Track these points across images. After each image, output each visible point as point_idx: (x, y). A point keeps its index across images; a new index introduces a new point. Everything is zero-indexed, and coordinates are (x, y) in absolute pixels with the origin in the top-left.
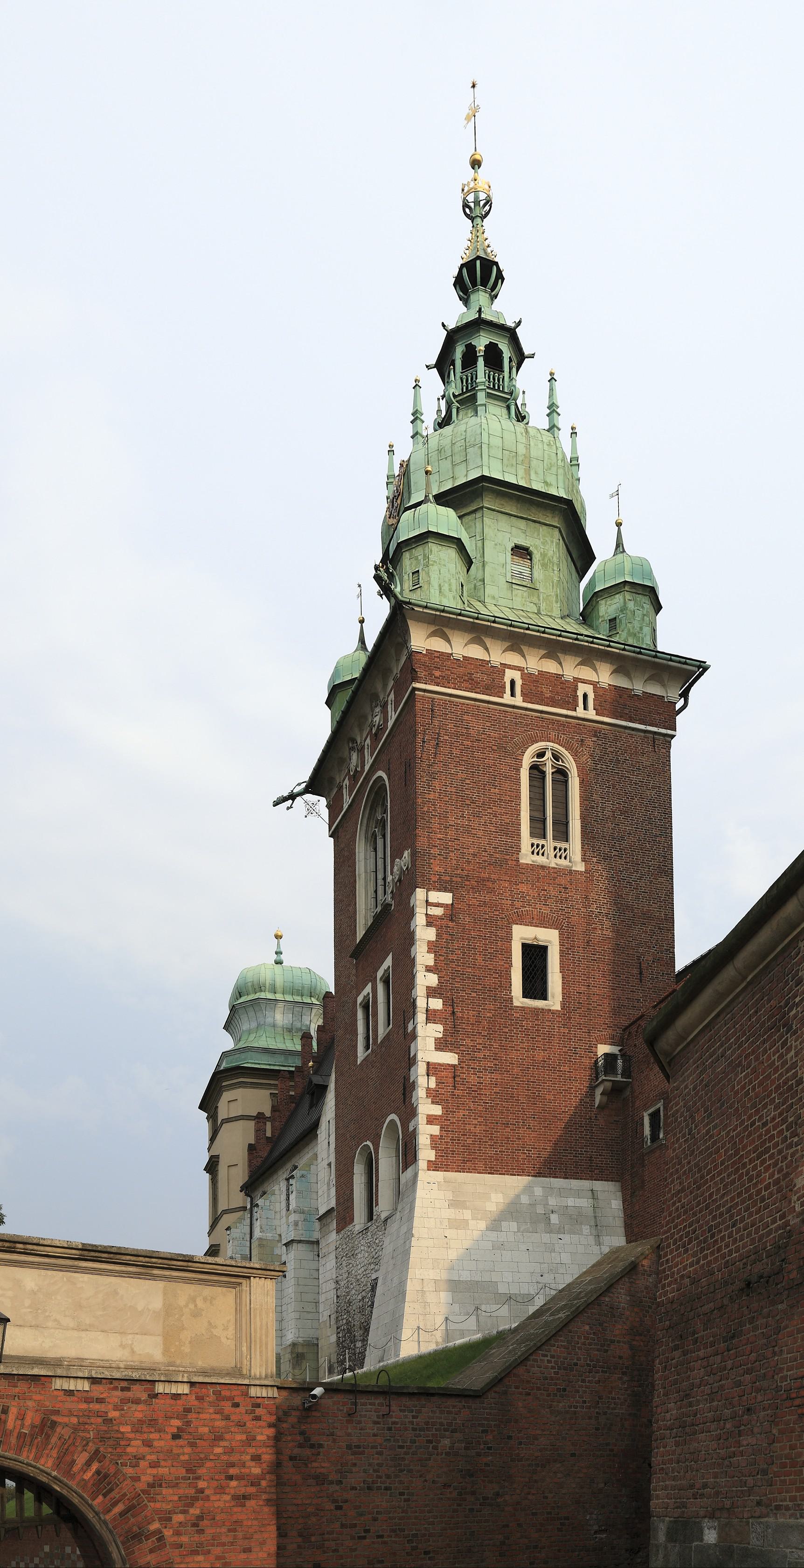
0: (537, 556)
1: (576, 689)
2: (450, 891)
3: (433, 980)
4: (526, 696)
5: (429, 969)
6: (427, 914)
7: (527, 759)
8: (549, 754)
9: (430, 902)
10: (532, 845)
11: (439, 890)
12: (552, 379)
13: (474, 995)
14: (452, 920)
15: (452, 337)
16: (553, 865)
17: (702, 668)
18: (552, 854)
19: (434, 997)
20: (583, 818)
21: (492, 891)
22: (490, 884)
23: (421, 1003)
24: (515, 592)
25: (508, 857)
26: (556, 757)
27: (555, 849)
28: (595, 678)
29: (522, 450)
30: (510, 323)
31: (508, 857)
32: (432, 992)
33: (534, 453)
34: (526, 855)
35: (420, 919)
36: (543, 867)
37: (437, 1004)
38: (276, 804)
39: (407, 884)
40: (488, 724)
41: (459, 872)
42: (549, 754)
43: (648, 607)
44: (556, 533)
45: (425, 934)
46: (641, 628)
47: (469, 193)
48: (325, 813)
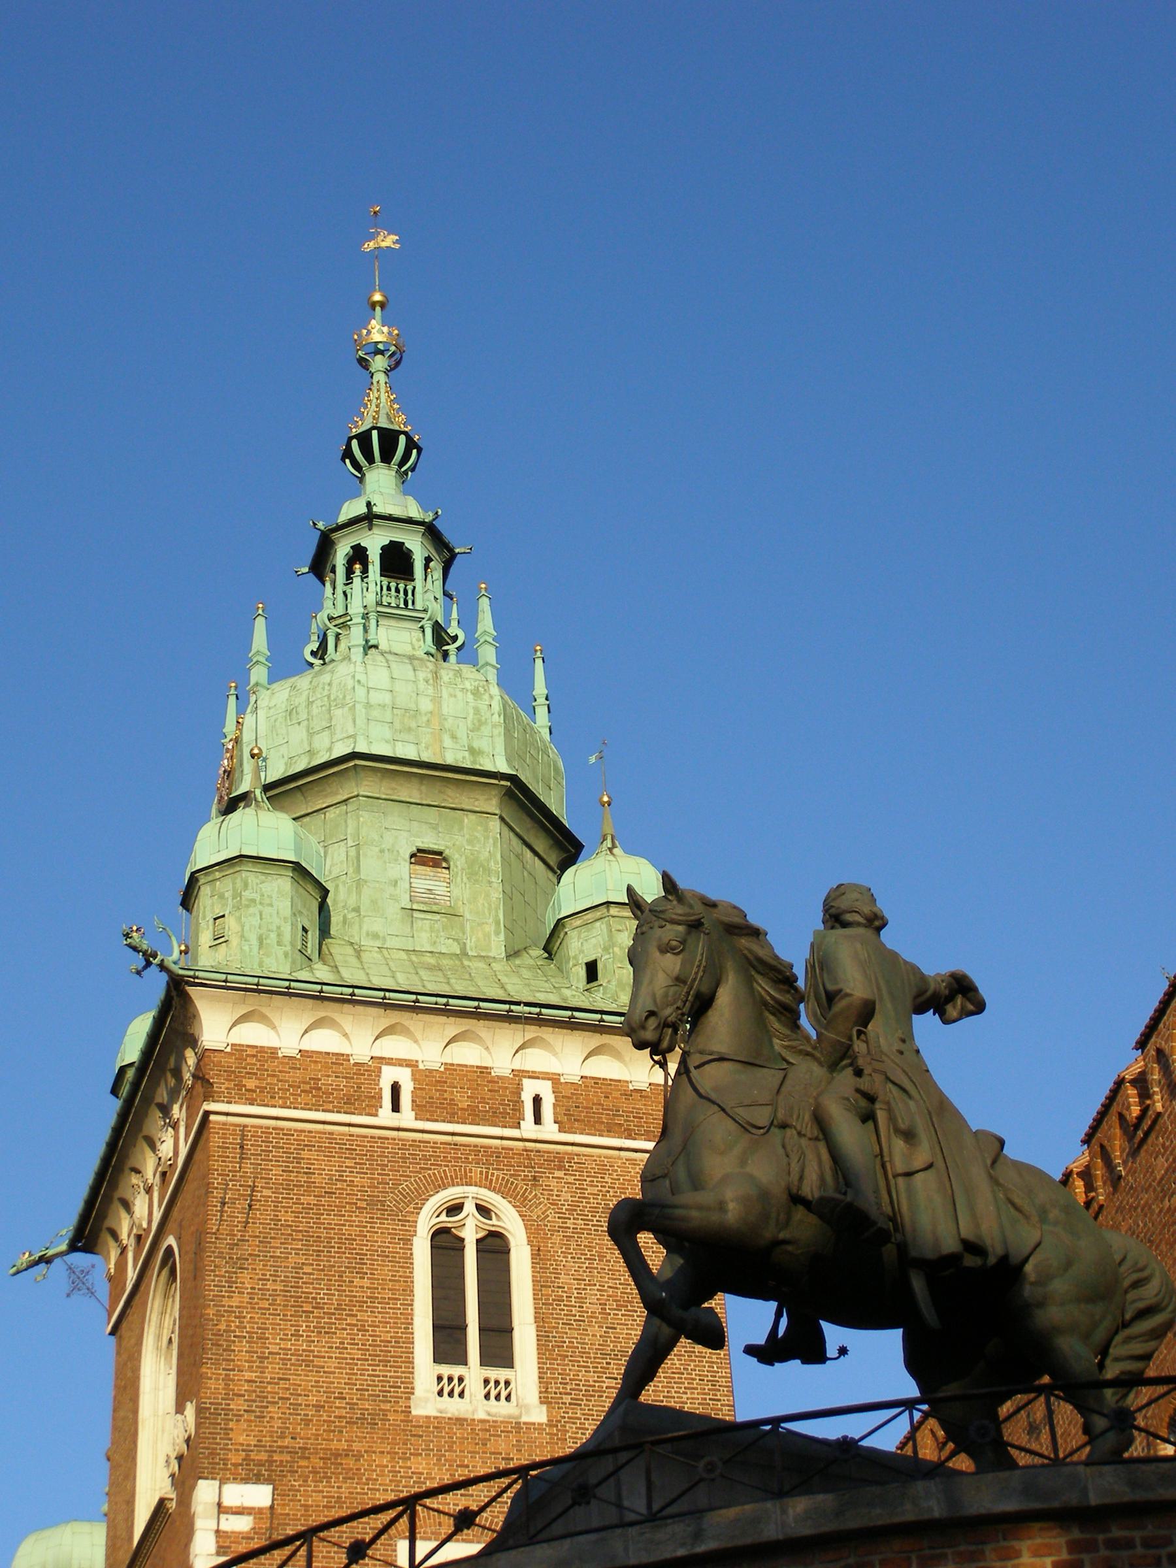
1: (519, 1089)
2: (268, 1481)
4: (421, 1110)
7: (426, 1221)
11: (246, 1480)
21: (352, 1475)
22: (350, 1462)
26: (484, 1210)
34: (427, 1400)
36: (460, 1421)
40: (349, 1163)
41: (287, 1441)
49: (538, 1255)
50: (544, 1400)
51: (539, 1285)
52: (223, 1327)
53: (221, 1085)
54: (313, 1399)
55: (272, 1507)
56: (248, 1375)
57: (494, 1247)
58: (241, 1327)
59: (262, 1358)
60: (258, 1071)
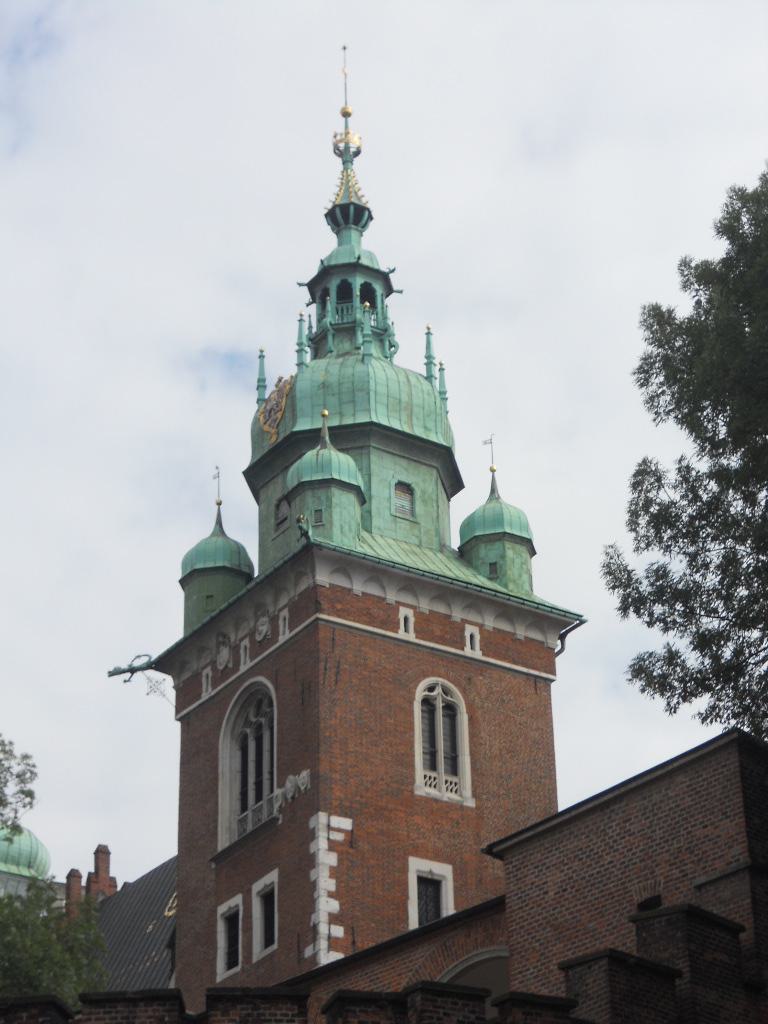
0: (418, 493)
2: (350, 817)
3: (334, 906)
5: (331, 895)
6: (328, 839)
7: (420, 692)
8: (438, 691)
9: (331, 827)
10: (425, 777)
11: (340, 815)
12: (428, 334)
13: (373, 925)
14: (352, 847)
15: (326, 271)
16: (445, 799)
17: (580, 621)
18: (444, 787)
19: (336, 924)
20: (472, 754)
22: (386, 813)
23: (323, 929)
24: (398, 525)
25: (403, 787)
26: (446, 691)
27: (446, 782)
28: (480, 621)
29: (405, 398)
30: (384, 268)
31: (403, 787)
32: (333, 919)
33: (415, 401)
34: (420, 787)
35: (322, 843)
36: (436, 801)
37: (338, 931)
38: (111, 674)
39: (305, 805)
40: (384, 656)
41: (358, 798)
42: (438, 691)
43: (526, 555)
44: (435, 472)
45: (327, 859)
46: (520, 576)
47: (341, 141)
48: (172, 694)
49: (471, 719)
50: (475, 795)
51: (472, 736)
52: (328, 734)
53: (325, 605)
54: (370, 779)
55: (352, 831)
56: (340, 762)
57: (451, 710)
58: (336, 736)
59: (347, 753)
60: (341, 599)
